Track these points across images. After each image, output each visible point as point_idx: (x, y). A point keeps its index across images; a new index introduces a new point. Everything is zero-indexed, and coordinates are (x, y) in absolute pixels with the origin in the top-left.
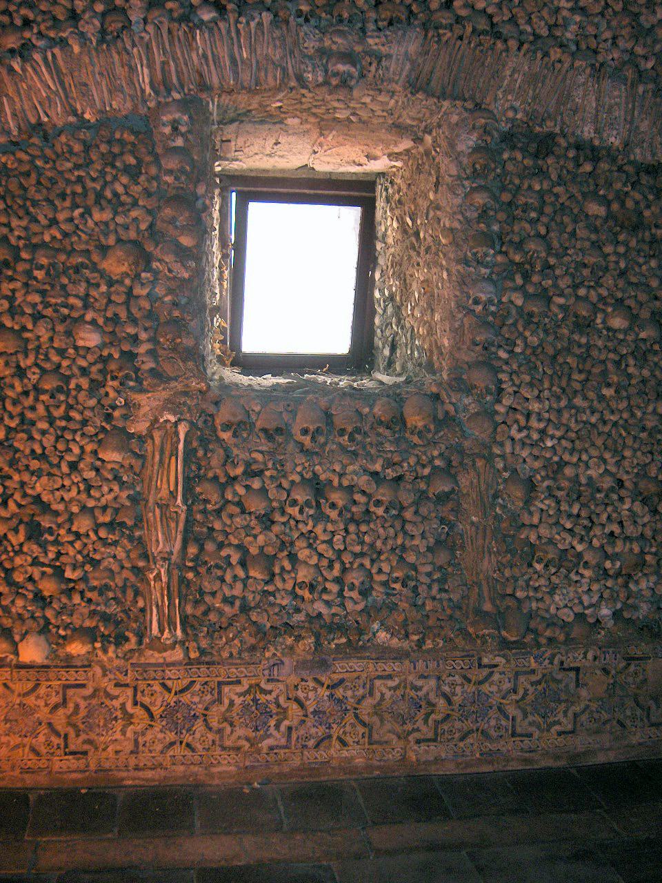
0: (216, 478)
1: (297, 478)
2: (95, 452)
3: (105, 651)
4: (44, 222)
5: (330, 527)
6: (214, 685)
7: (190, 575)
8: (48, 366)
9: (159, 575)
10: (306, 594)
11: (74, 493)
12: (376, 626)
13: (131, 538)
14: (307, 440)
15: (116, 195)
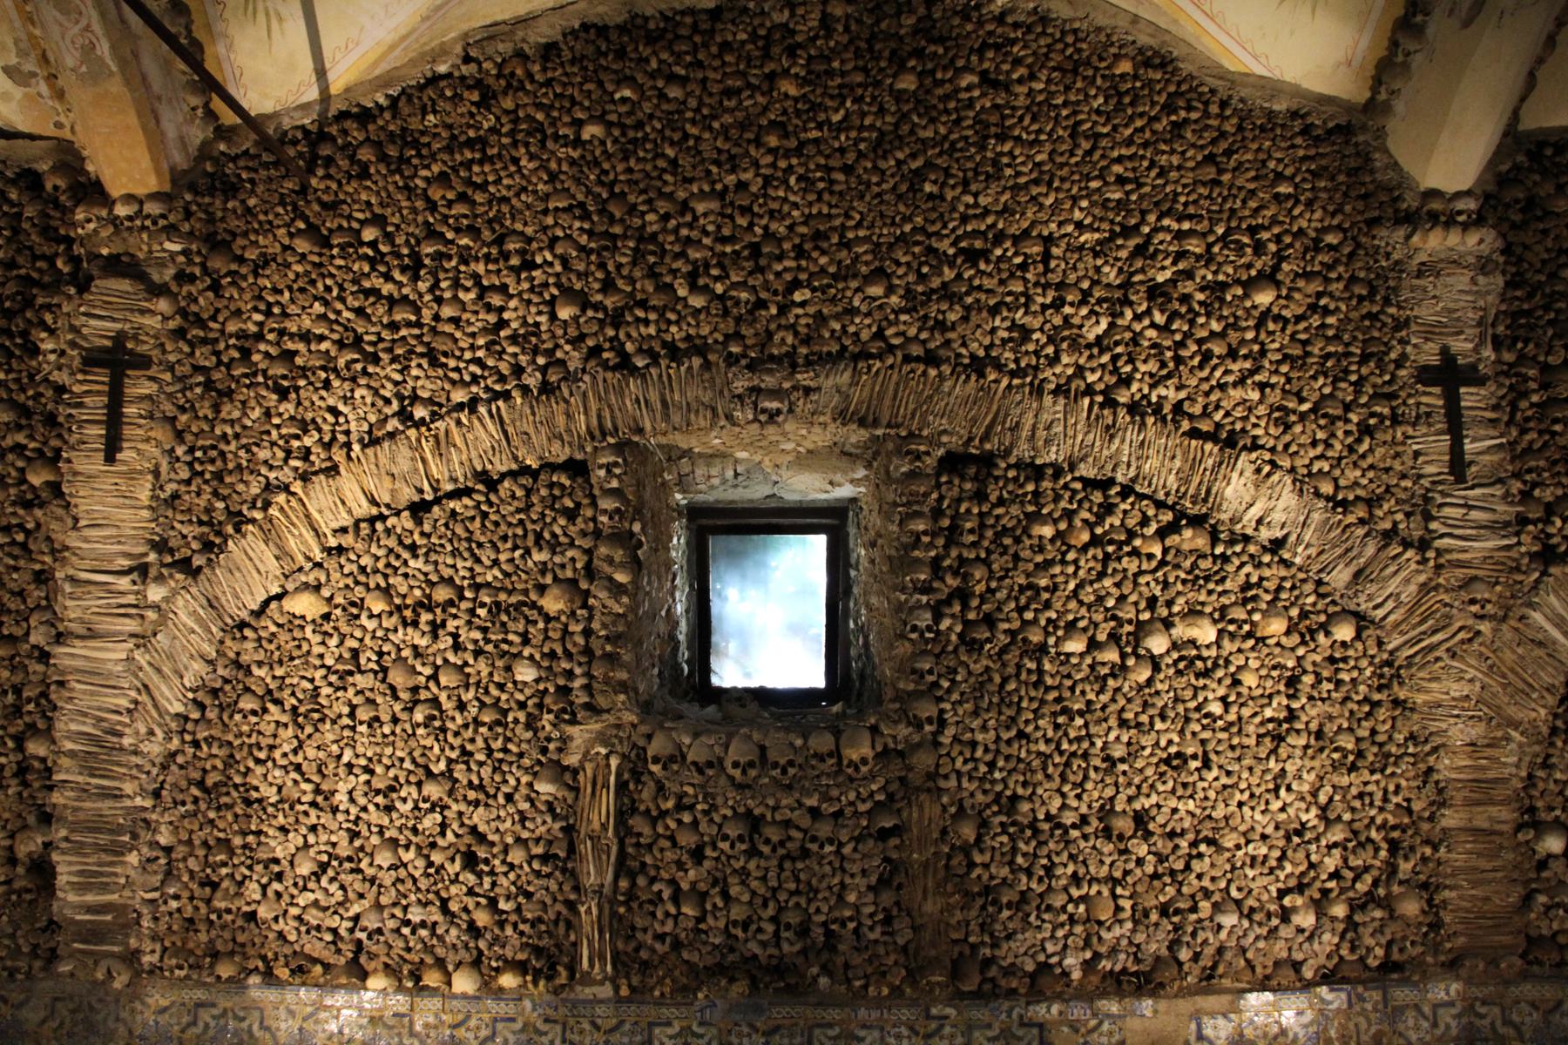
0: (648, 811)
1: (729, 813)
2: (530, 785)
3: (535, 983)
4: (488, 563)
5: (763, 863)
6: (644, 1025)
7: (622, 910)
8: (488, 700)
9: (589, 909)
10: (739, 932)
11: (508, 824)
12: (815, 970)
13: (564, 871)
14: (737, 773)
15: (554, 535)
